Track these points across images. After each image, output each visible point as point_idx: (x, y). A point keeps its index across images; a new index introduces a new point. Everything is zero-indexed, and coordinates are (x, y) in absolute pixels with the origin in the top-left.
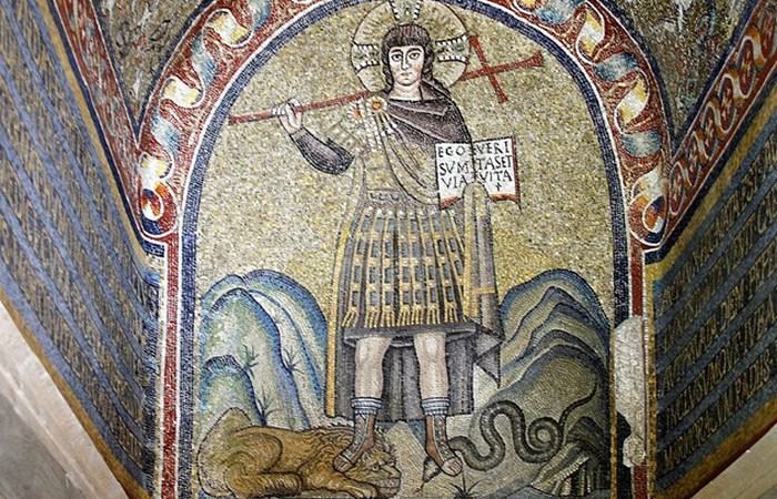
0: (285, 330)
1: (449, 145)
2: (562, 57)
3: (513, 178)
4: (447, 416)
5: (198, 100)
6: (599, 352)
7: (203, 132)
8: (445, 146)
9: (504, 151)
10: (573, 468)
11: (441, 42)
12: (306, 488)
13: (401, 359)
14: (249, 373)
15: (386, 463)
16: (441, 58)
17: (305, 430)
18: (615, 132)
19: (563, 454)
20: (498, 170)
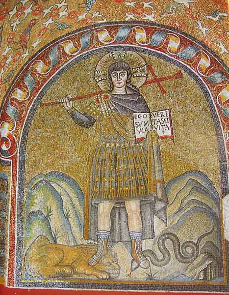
0: (64, 198)
1: (139, 114)
2: (191, 73)
3: (170, 128)
4: (142, 240)
5: (27, 96)
6: (216, 210)
7: (29, 111)
8: (138, 114)
9: (165, 116)
10: (204, 266)
11: (135, 68)
12: (76, 273)
13: (119, 212)
14: (48, 219)
15: (113, 262)
16: (135, 76)
17: (74, 246)
18: (218, 106)
19: (199, 259)
20: (163, 125)
